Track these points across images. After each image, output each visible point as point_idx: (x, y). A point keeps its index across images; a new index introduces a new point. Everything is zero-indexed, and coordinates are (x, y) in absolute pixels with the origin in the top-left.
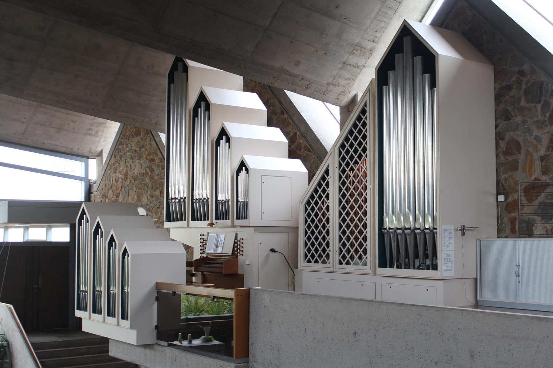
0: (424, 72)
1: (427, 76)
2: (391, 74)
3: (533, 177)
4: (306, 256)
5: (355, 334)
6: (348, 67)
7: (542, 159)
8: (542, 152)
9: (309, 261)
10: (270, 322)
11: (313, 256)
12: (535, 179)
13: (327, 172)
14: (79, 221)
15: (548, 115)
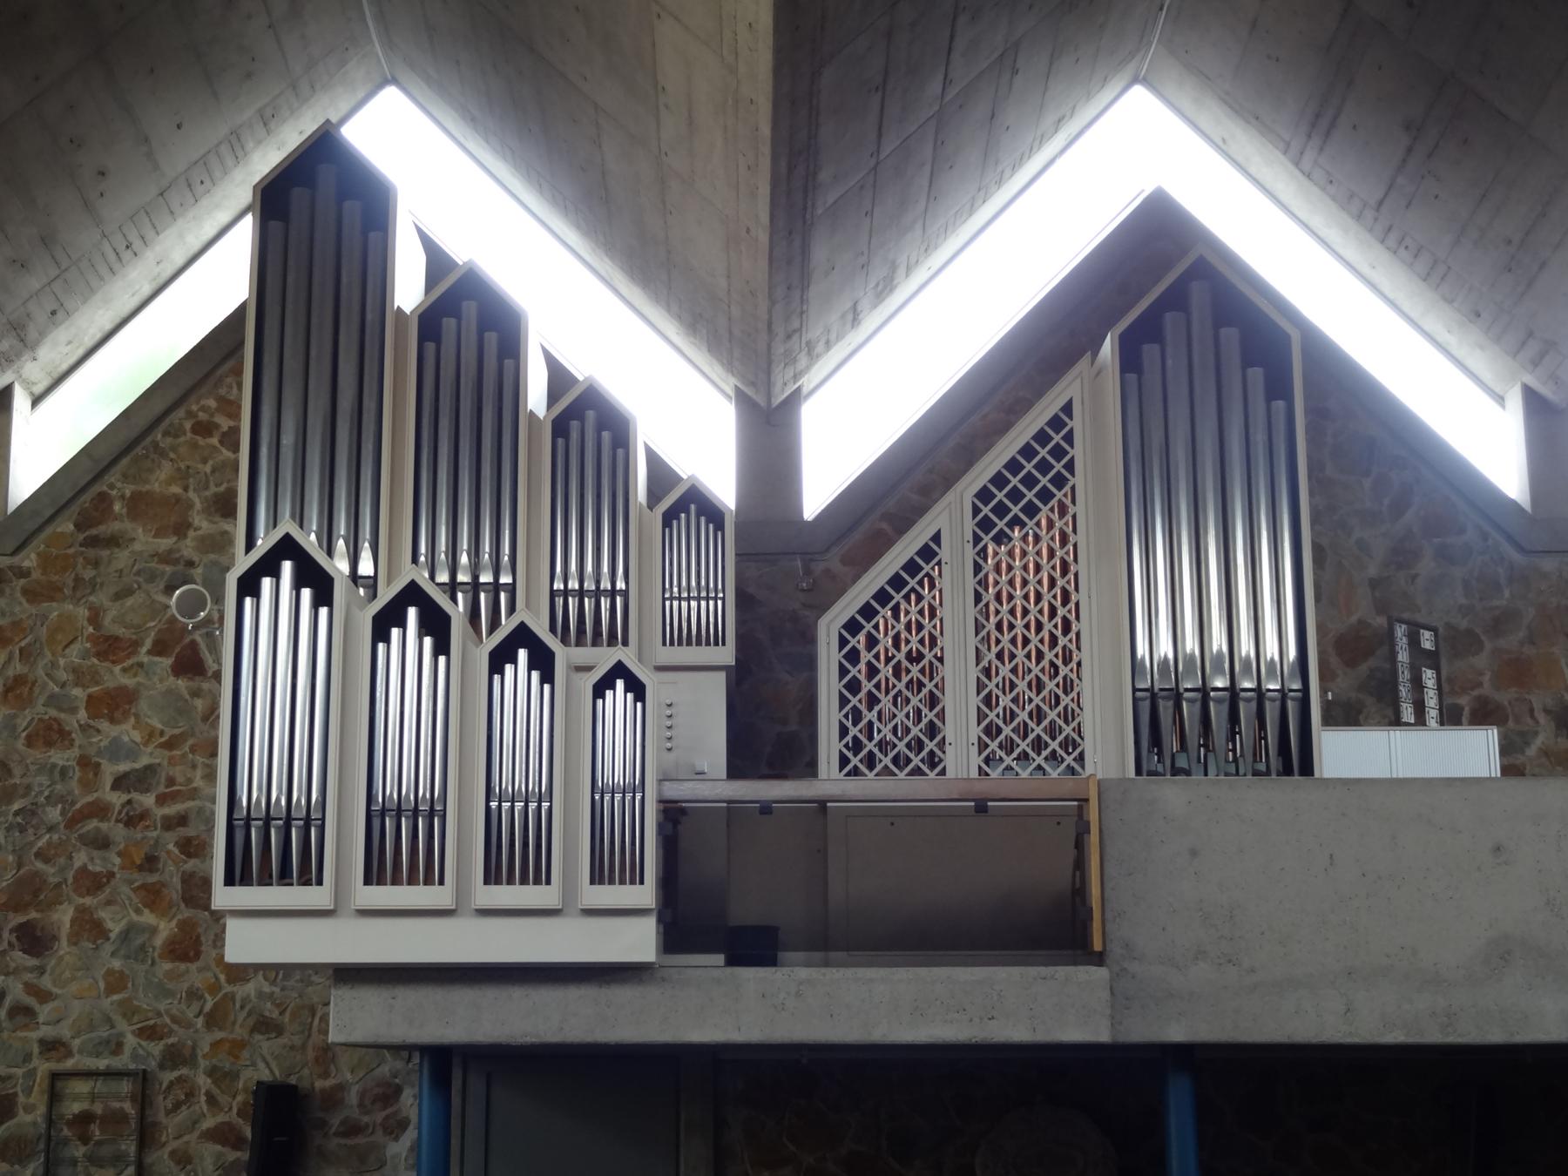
0: (1247, 363)
1: (1256, 374)
2: (1150, 351)
3: (1354, 619)
4: (844, 761)
5: (1498, 849)
6: (850, 317)
7: (1374, 584)
8: (1372, 571)
9: (855, 772)
10: (1194, 853)
11: (870, 761)
12: (1360, 622)
13: (927, 553)
14: (240, 580)
15: (1386, 501)
